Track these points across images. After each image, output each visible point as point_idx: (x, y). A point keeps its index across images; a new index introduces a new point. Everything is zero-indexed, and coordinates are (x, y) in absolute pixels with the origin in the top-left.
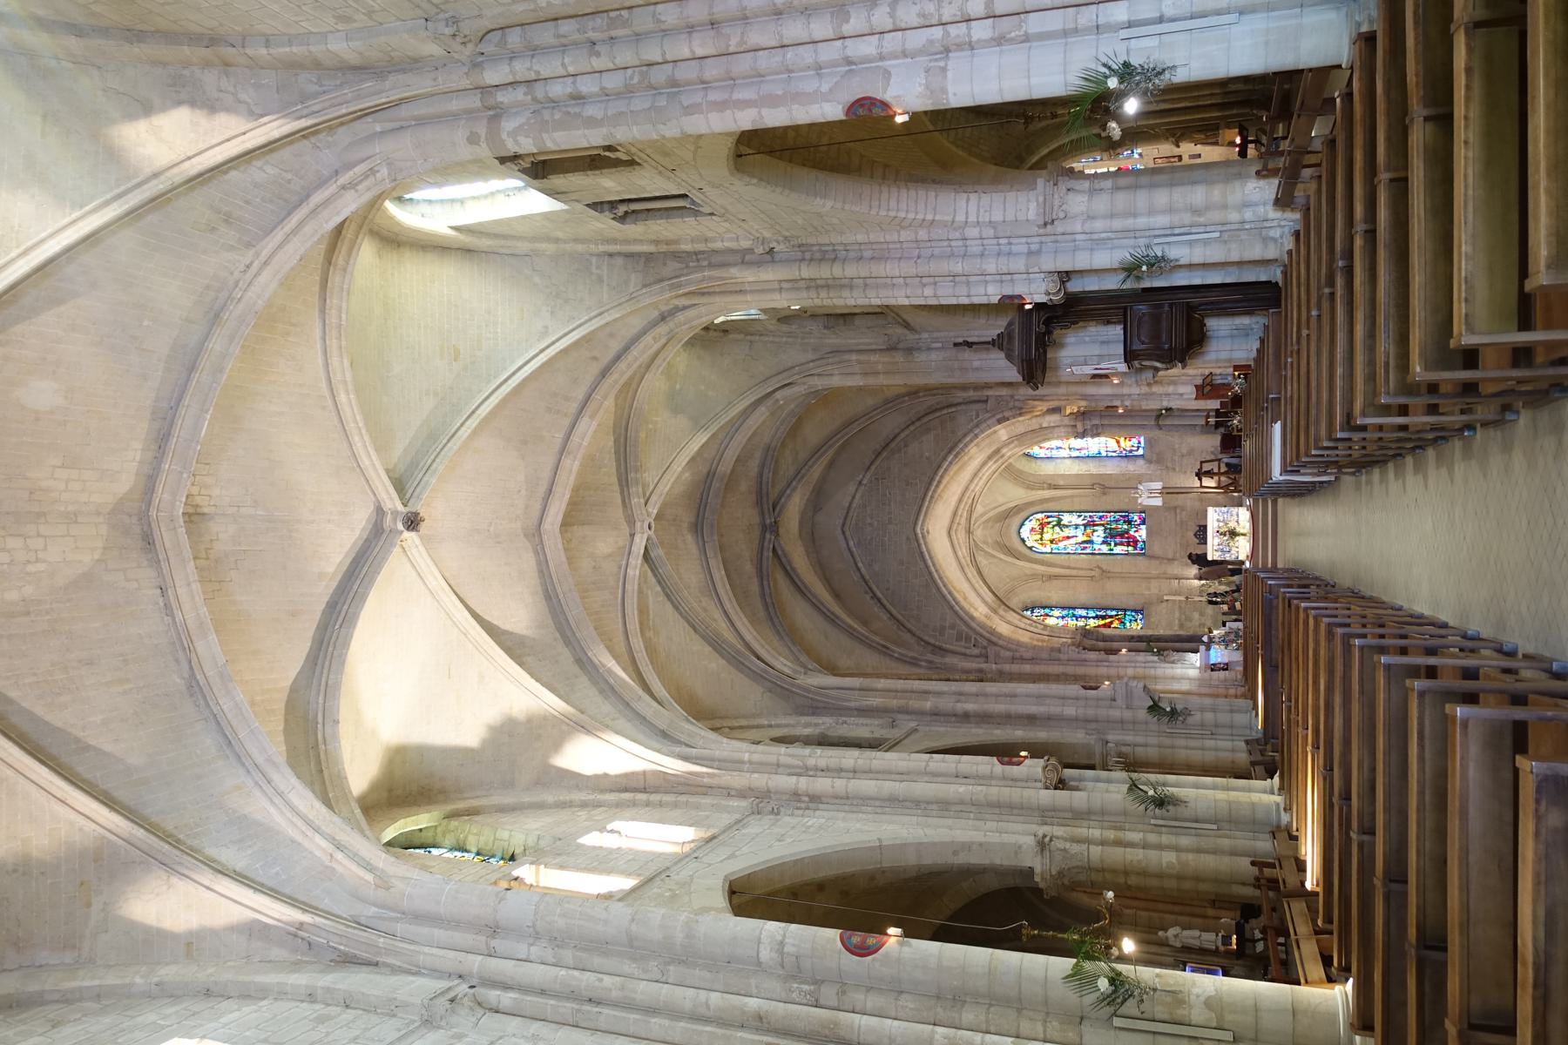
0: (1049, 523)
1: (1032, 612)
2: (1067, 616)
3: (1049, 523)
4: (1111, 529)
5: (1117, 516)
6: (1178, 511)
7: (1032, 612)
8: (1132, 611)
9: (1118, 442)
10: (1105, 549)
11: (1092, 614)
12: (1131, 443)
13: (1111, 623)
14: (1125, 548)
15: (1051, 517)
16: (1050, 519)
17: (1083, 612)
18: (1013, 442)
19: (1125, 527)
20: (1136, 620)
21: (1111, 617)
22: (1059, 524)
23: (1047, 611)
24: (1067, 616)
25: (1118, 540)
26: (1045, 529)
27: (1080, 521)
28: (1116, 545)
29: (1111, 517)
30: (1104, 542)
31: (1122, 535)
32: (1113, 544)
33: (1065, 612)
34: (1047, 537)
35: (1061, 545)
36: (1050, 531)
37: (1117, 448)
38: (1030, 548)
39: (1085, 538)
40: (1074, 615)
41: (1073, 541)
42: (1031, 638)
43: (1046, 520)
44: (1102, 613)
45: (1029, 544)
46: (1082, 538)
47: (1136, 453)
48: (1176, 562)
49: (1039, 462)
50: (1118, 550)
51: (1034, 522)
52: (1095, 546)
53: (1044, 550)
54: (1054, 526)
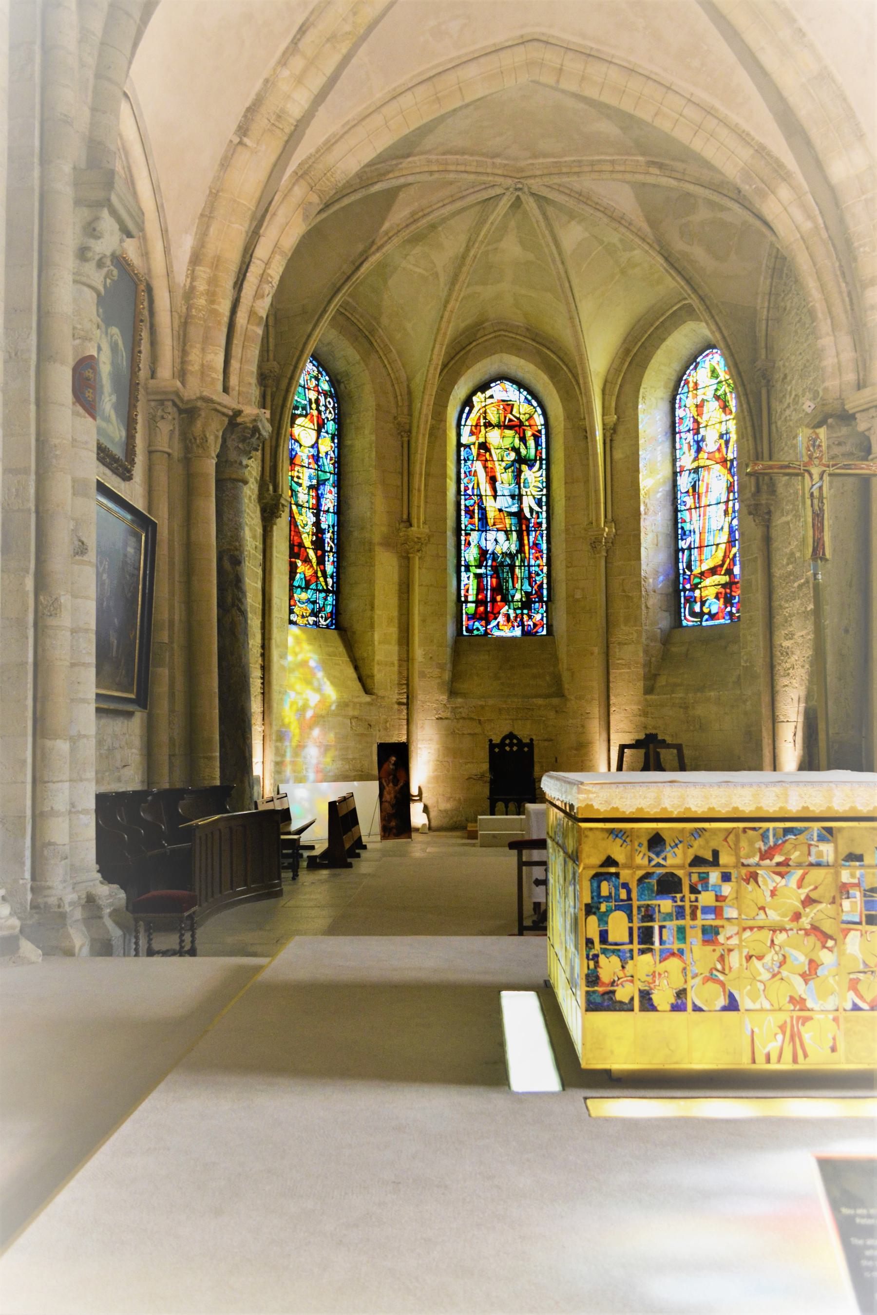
0: (523, 439)
1: (326, 394)
2: (320, 468)
3: (523, 439)
4: (512, 567)
5: (542, 579)
6: (555, 701)
7: (326, 394)
8: (336, 606)
9: (713, 571)
10: (470, 555)
11: (327, 521)
12: (712, 599)
13: (307, 561)
14: (471, 598)
15: (537, 444)
16: (531, 443)
17: (329, 501)
18: (810, 217)
19: (518, 597)
20: (314, 614)
21: (321, 561)
22: (521, 460)
23: (331, 426)
24: (320, 468)
25: (489, 582)
26: (509, 433)
27: (528, 502)
28: (478, 576)
29: (538, 564)
30: (483, 553)
31: (497, 590)
32: (479, 571)
33: (328, 466)
34: (494, 437)
35: (478, 466)
36: (507, 443)
37: (697, 571)
38: (468, 403)
39: (491, 514)
40: (321, 483)
41: (485, 488)
42: (241, 327)
43: (529, 433)
44: (329, 544)
45: (478, 399)
46: (491, 506)
47: (685, 612)
48: (444, 698)
49: (665, 406)
50: (469, 582)
51: (525, 408)
52: (474, 537)
53: (465, 431)
54: (517, 451)
